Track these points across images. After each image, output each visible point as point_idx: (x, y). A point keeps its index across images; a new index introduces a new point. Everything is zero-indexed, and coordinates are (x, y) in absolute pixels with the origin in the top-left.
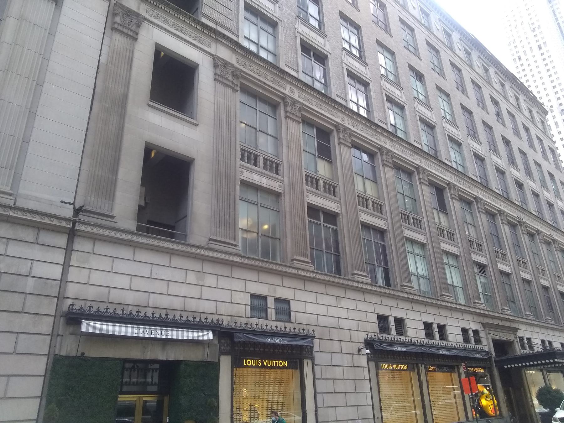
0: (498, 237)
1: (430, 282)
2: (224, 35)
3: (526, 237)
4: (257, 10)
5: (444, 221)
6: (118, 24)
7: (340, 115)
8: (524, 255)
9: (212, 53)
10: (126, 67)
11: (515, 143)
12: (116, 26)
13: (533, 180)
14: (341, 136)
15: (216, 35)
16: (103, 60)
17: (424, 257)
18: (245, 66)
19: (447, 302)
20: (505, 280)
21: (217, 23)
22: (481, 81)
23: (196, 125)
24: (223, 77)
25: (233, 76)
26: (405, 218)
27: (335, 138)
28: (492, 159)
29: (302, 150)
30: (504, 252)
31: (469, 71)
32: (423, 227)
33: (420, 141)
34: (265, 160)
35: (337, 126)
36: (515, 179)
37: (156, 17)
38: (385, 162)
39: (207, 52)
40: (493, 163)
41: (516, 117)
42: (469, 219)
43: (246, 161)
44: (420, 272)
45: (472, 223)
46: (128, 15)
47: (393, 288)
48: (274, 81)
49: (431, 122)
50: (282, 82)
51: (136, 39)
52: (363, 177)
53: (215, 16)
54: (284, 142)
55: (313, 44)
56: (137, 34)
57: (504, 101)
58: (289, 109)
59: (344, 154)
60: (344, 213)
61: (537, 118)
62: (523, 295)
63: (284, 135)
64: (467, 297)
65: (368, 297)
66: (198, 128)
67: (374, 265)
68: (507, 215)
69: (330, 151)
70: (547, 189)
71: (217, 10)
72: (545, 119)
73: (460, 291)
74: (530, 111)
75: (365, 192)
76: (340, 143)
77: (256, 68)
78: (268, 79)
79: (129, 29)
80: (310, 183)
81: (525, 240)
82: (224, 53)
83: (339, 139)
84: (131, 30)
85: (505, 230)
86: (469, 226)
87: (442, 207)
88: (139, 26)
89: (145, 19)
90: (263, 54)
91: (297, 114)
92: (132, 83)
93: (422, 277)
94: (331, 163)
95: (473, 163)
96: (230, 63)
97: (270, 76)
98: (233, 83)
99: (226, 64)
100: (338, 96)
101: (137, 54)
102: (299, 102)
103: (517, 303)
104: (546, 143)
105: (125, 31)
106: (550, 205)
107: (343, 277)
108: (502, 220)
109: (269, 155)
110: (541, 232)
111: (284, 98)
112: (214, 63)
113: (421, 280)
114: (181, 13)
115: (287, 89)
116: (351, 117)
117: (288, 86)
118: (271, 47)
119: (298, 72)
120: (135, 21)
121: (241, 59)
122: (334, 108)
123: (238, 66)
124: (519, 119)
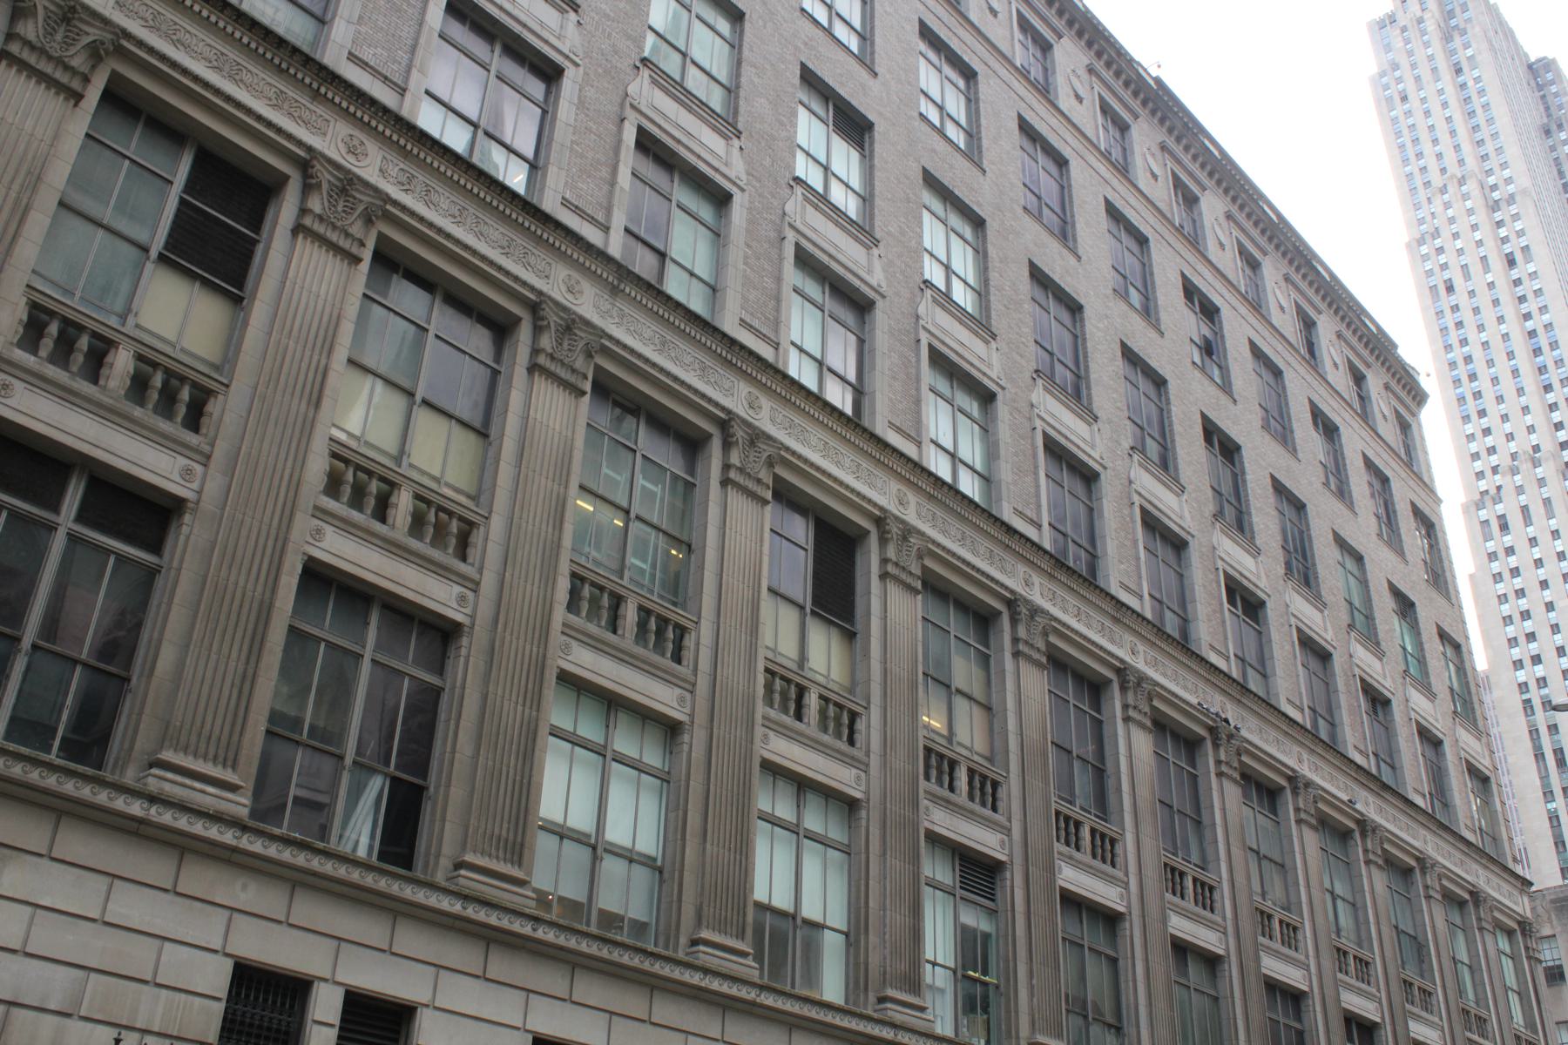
0: (1100, 773)
1: (662, 881)
3: (1233, 792)
5: (824, 656)
7: (342, 129)
8: (1209, 851)
11: (1261, 458)
13: (1318, 601)
14: (315, 204)
17: (664, 778)
19: (706, 971)
20: (1090, 935)
22: (1152, 220)
26: (595, 597)
27: (286, 211)
28: (1129, 483)
29: (46, 202)
30: (1110, 829)
31: (1108, 175)
32: (688, 655)
33: (777, 331)
35: (307, 162)
36: (1228, 576)
38: (542, 360)
40: (1136, 498)
41: (1288, 375)
42: (963, 672)
44: (617, 832)
45: (978, 693)
47: (418, 873)
49: (857, 283)
52: (411, 394)
57: (1243, 310)
59: (299, 273)
60: (208, 504)
61: (1381, 404)
62: (1161, 1005)
64: (857, 978)
65: (198, 877)
67: (341, 758)
68: (1154, 692)
69: (247, 257)
70: (1372, 640)
72: (1413, 415)
73: (832, 948)
74: (1359, 379)
76: (298, 229)
81: (1226, 802)
83: (303, 211)
85: (1135, 749)
86: (961, 704)
87: (834, 597)
93: (630, 857)
94: (237, 300)
95: (1036, 474)
100: (353, 58)
102: (106, 21)
103: (1129, 1029)
104: (1402, 492)
106: (1378, 702)
107: (109, 777)
108: (1125, 707)
110: (1308, 784)
113: (612, 867)
116: (405, 154)
122: (316, 95)
124: (1300, 387)
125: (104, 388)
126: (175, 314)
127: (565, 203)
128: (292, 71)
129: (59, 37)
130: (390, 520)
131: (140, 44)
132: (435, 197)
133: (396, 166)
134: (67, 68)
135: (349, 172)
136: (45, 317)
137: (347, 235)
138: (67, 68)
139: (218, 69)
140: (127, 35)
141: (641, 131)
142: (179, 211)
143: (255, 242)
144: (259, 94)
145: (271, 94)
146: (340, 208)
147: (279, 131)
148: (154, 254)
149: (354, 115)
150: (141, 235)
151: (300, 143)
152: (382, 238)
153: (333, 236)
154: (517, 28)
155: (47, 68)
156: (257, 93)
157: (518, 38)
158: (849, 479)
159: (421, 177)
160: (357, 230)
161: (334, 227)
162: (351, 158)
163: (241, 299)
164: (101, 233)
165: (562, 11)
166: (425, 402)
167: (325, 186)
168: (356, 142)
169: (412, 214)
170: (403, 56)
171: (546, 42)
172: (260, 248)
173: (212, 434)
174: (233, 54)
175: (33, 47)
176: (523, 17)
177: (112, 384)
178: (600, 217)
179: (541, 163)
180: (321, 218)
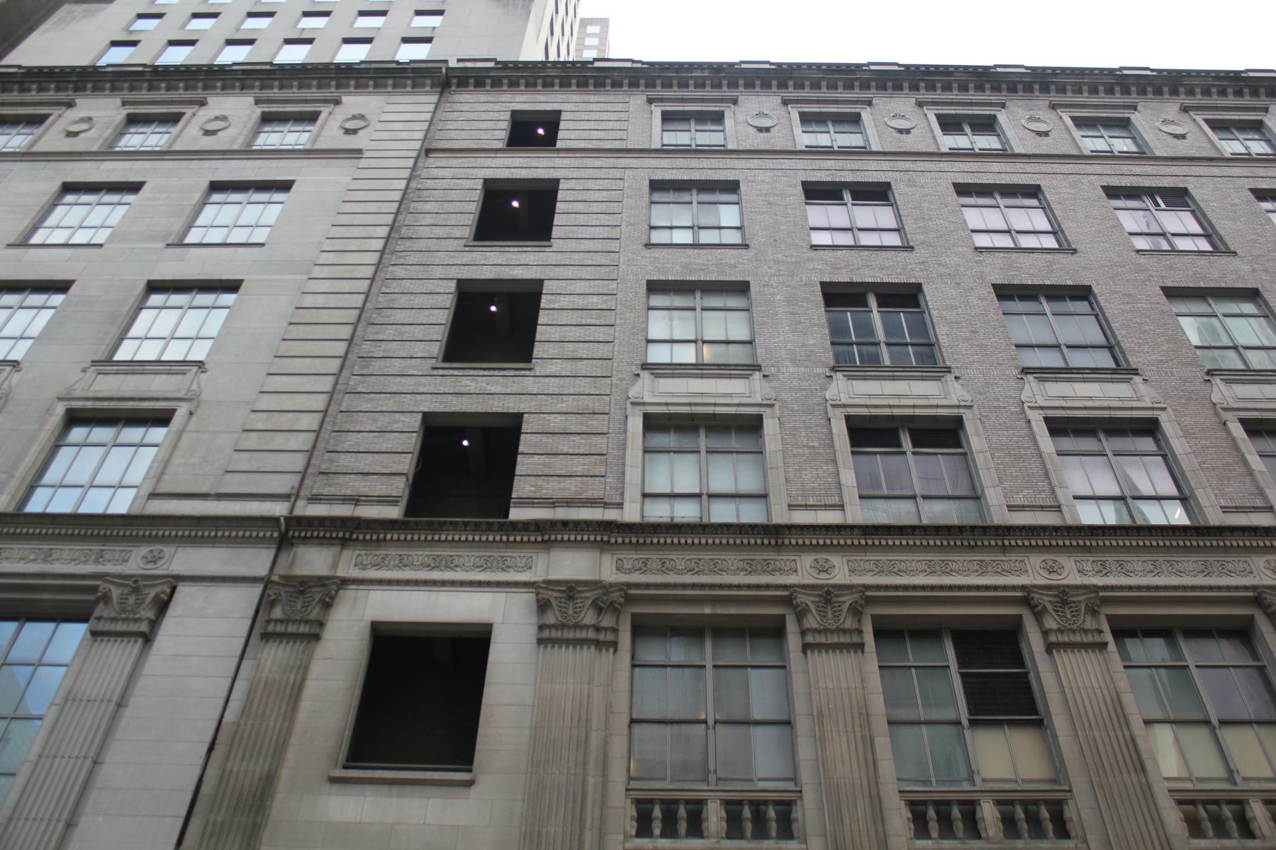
2: (565, 523)
4: (692, 417)
6: (276, 621)
7: (1035, 560)
9: (534, 579)
10: (283, 710)
12: (271, 628)
14: (1050, 623)
15: (546, 534)
16: (230, 716)
18: (644, 568)
21: (553, 503)
23: (469, 784)
24: (563, 626)
25: (600, 610)
27: (1034, 640)
34: (732, 809)
35: (1026, 597)
37: (377, 566)
39: (517, 584)
43: (657, 831)
46: (302, 592)
48: (751, 568)
50: (783, 558)
51: (317, 637)
52: (1207, 722)
53: (551, 488)
54: (803, 726)
55: (897, 412)
56: (321, 625)
58: (811, 622)
59: (1070, 679)
63: (800, 706)
66: (474, 790)
71: (558, 472)
75: (1231, 775)
76: (1050, 648)
77: (680, 559)
78: (733, 571)
79: (300, 621)
80: (934, 827)
82: (571, 565)
83: (1045, 633)
84: (306, 622)
88: (327, 605)
89: (345, 582)
90: (722, 513)
91: (848, 625)
92: (294, 740)
96: (586, 583)
97: (732, 559)
98: (598, 629)
99: (571, 589)
100: (1012, 508)
101: (316, 669)
102: (850, 587)
105: (292, 628)
109: (762, 785)
111: (788, 597)
112: (538, 601)
114: (441, 527)
115: (803, 570)
116: (1089, 550)
117: (807, 560)
118: (749, 483)
119: (841, 507)
120: (317, 597)
121: (630, 557)
122: (1005, 549)
123: (623, 578)
125: (987, 838)
126: (1003, 758)
127: (1225, 509)
128: (979, 543)
129: (830, 616)
130: (1258, 833)
131: (878, 587)
132: (1129, 567)
133: (1088, 562)
134: (845, 631)
135: (1058, 587)
136: (921, 808)
137: (1086, 631)
138: (845, 631)
139: (932, 573)
140: (867, 587)
141: (1244, 422)
142: (964, 683)
143: (1026, 675)
144: (967, 572)
145: (976, 567)
146: (1069, 616)
147: (996, 588)
148: (965, 722)
150: (949, 714)
151: (1014, 588)
152: (1110, 618)
153: (1077, 638)
155: (834, 639)
156: (967, 573)
157: (1111, 419)
159: (1110, 559)
160: (1089, 624)
161: (1074, 631)
162: (1053, 576)
163: (1041, 721)
164: (924, 728)
165: (1128, 381)
166: (1223, 723)
167: (1049, 607)
168: (1050, 563)
169: (1121, 588)
170: (1043, 485)
171: (1132, 409)
172: (1032, 676)
173: (1080, 833)
174: (936, 557)
175: (818, 631)
176: (1105, 404)
177: (991, 832)
178: (1259, 503)
179: (1187, 493)
180: (1060, 631)
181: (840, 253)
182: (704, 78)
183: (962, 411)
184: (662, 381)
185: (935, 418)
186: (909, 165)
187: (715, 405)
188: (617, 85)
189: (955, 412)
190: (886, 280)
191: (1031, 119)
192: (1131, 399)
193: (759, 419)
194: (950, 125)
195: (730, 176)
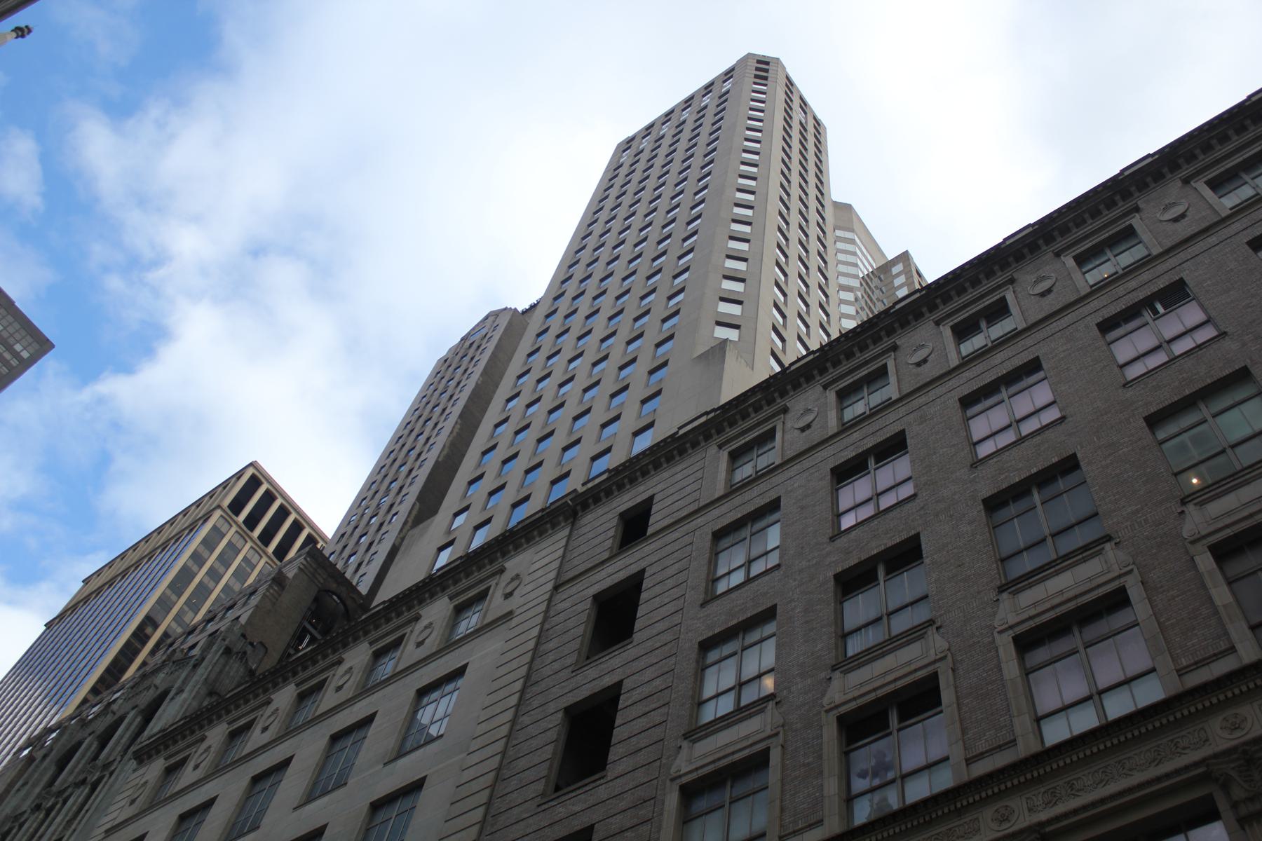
55: (880, 693)
116: (1039, 780)
122: (959, 812)
149: (994, 793)
154: (1071, 606)
158: (1113, 788)
162: (1005, 826)
171: (1099, 586)
181: (854, 533)
182: (760, 400)
183: (1122, 580)
184: (850, 675)
185: (916, 683)
186: (923, 400)
187: (874, 690)
188: (695, 445)
189: (930, 669)
190: (890, 544)
191: (1166, 209)
192: (1102, 574)
193: (1122, 591)
194: (963, 332)
195: (888, 433)
